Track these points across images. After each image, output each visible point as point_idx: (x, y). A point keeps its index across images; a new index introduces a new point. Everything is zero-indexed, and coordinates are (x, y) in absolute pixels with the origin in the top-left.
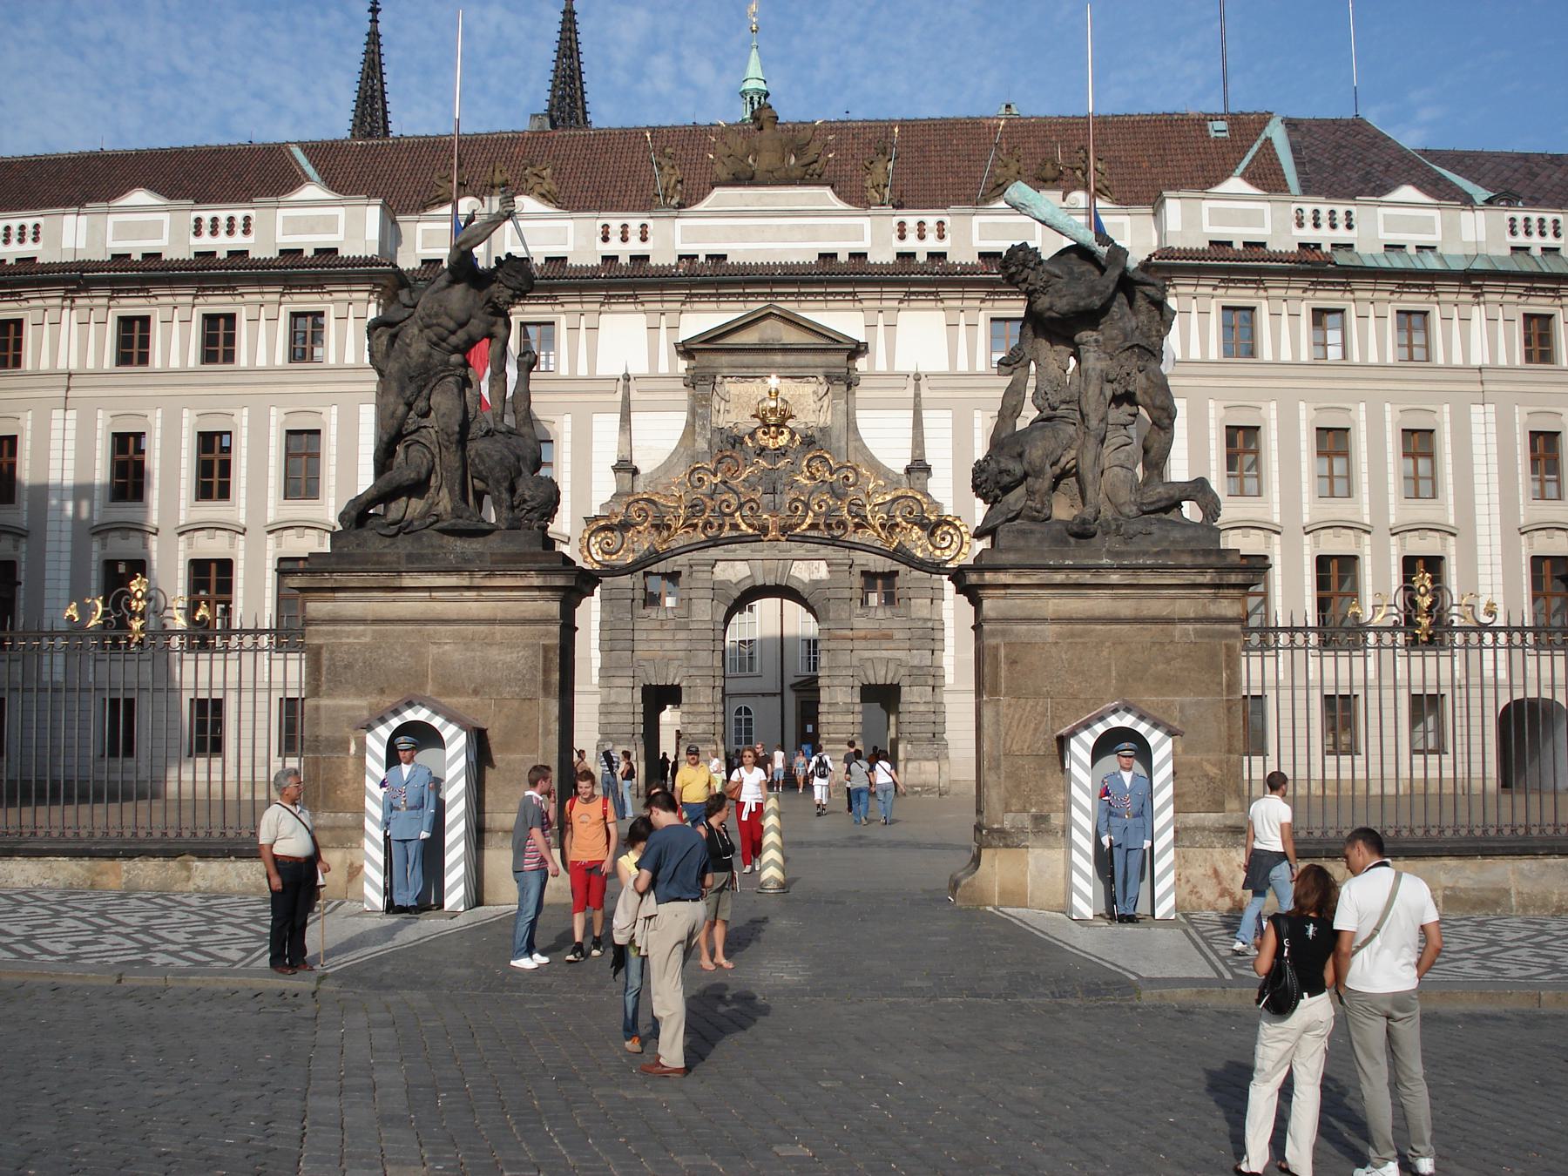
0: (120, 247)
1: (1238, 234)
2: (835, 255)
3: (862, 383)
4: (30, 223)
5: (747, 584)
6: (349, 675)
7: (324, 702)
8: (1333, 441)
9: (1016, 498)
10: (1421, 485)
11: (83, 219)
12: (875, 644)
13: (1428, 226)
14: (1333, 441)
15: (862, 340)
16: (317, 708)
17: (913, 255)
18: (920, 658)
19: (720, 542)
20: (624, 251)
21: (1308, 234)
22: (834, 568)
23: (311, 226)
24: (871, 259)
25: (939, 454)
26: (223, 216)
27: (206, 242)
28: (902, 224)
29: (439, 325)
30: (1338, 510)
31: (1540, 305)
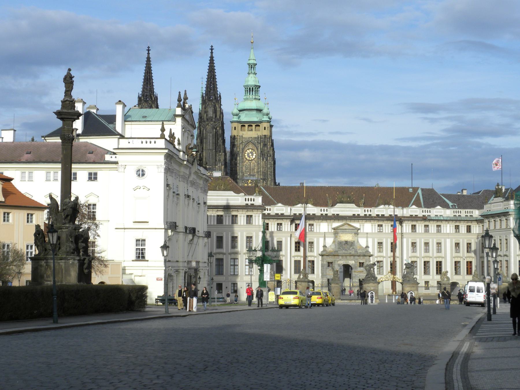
1: (414, 214)
3: (359, 234)
8: (427, 244)
9: (405, 279)
10: (439, 250)
12: (361, 273)
13: (441, 212)
14: (427, 244)
15: (359, 228)
17: (366, 215)
20: (324, 213)
21: (424, 214)
24: (361, 215)
25: (370, 245)
28: (365, 210)
30: (427, 254)
31: (457, 224)
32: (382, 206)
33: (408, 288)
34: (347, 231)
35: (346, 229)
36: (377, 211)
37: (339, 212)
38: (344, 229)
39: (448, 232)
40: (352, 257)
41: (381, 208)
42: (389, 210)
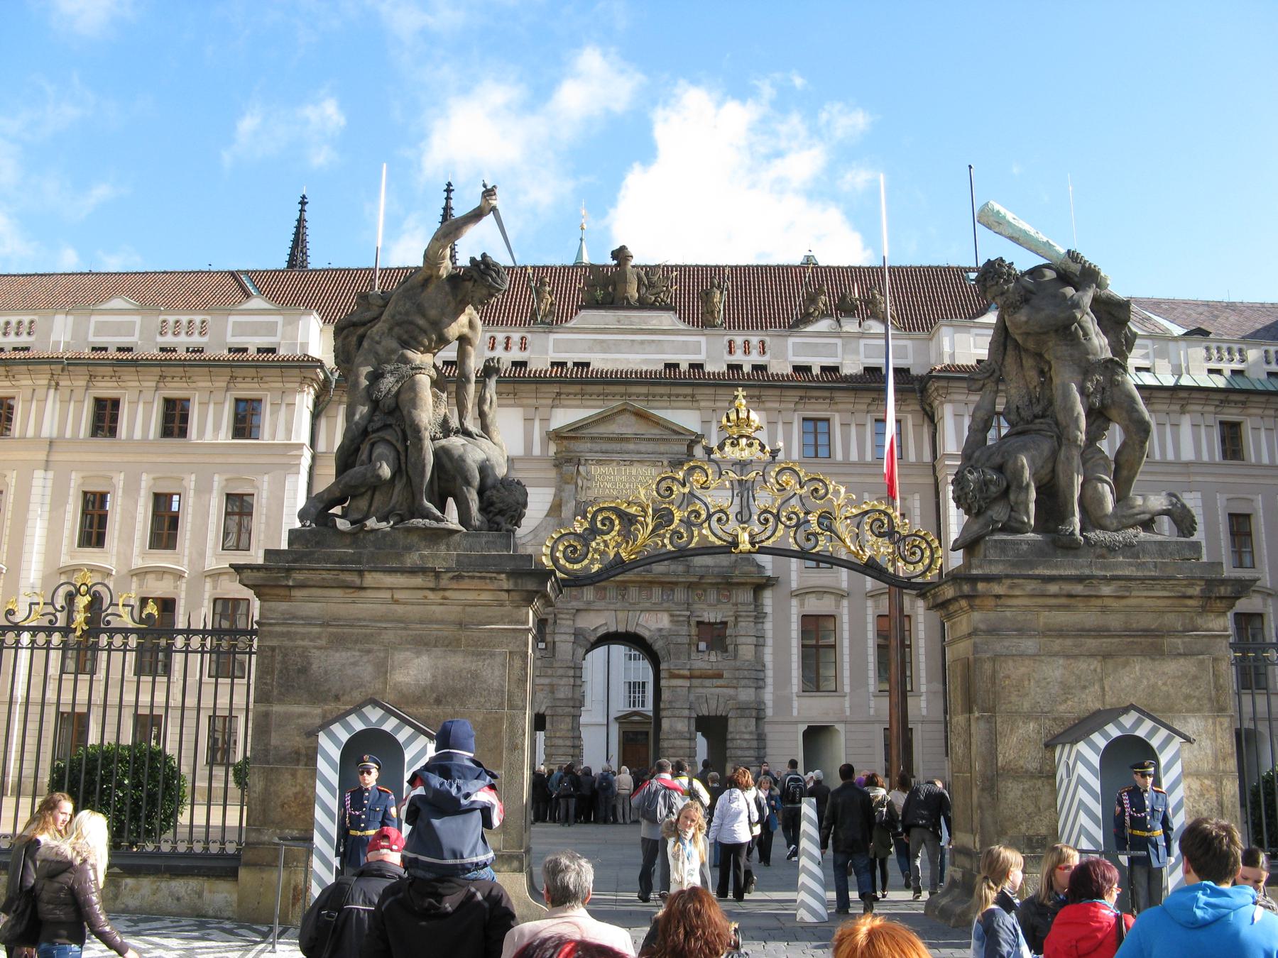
0: (100, 340)
2: (676, 366)
4: (26, 319)
5: (601, 632)
6: (302, 680)
7: (277, 708)
9: (999, 513)
11: (71, 319)
12: (707, 682)
16: (266, 715)
17: (739, 367)
18: (746, 695)
19: (688, 553)
22: (675, 618)
23: (255, 330)
24: (709, 368)
26: (184, 319)
27: (169, 340)
29: (411, 323)
31: (1231, 415)
32: (824, 325)
33: (1055, 671)
34: (631, 446)
35: (622, 439)
36: (798, 350)
37: (591, 350)
38: (610, 439)
39: (1188, 454)
40: (657, 593)
41: (819, 334)
42: (862, 342)
